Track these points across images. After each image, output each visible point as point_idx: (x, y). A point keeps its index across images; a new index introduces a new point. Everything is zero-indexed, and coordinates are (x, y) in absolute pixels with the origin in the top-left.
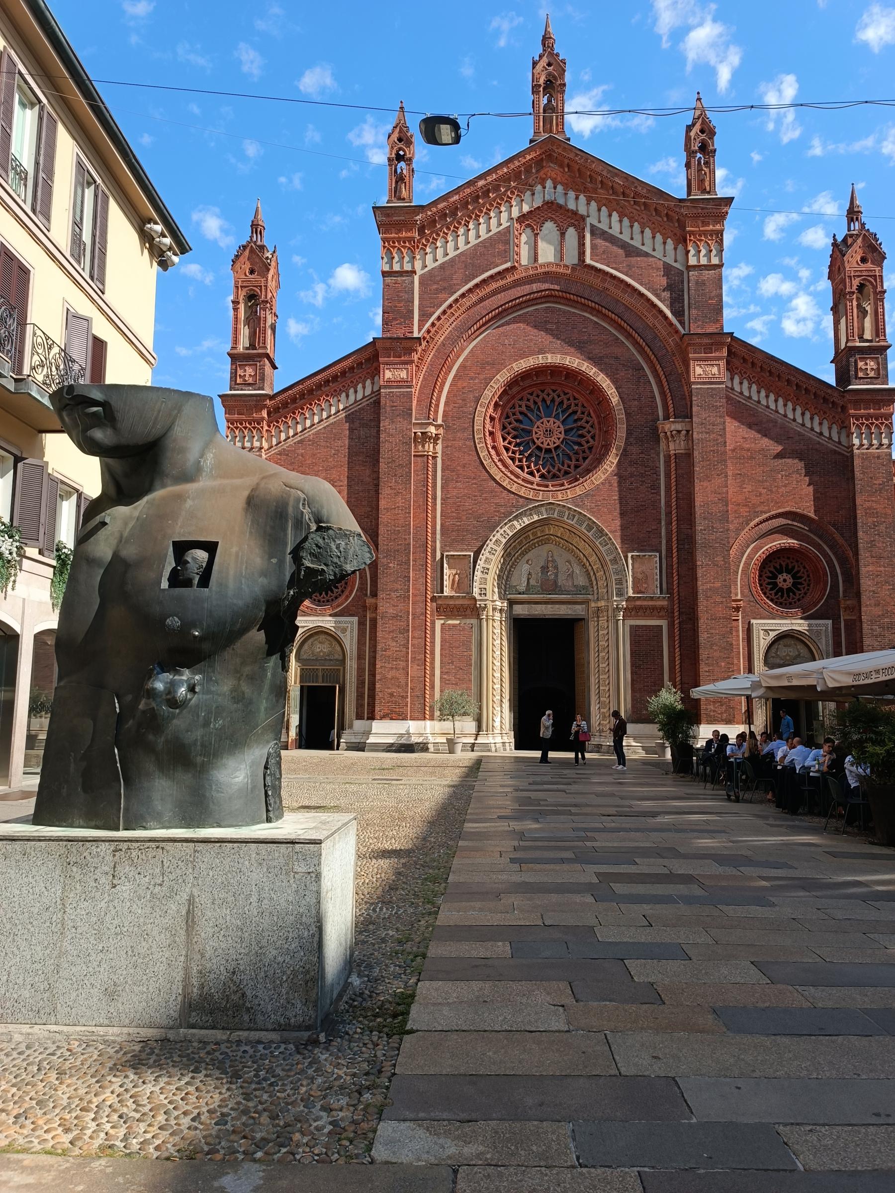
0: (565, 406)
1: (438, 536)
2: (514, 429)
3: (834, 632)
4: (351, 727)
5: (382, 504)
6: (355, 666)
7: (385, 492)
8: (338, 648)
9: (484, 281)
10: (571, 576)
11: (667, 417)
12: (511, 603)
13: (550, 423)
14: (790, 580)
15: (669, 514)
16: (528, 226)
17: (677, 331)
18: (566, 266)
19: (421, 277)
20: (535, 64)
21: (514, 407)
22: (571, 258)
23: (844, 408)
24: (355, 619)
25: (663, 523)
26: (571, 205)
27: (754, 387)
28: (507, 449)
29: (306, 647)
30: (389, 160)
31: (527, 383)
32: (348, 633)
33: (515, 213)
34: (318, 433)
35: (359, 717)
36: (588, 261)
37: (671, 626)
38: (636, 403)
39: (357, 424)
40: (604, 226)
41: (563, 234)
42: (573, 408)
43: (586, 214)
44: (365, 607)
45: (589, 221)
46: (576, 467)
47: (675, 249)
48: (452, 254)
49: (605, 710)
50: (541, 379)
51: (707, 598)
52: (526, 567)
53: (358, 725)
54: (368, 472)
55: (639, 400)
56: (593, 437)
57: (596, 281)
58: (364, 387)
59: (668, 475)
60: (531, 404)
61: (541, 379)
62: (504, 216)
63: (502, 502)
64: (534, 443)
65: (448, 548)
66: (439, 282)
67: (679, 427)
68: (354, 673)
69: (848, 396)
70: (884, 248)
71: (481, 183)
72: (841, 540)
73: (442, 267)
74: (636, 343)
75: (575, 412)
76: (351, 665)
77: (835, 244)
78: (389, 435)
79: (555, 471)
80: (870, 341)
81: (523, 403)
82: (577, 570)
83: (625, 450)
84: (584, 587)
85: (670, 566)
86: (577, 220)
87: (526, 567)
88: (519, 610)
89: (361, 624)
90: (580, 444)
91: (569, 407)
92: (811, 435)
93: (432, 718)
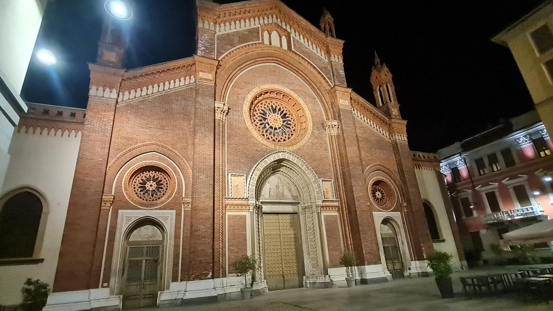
4: (168, 288)
19: (218, 36)
22: (285, 46)
24: (174, 212)
26: (284, 27)
32: (169, 220)
34: (155, 98)
35: (175, 279)
36: (293, 50)
39: (180, 98)
40: (297, 38)
41: (280, 37)
48: (233, 30)
49: (314, 262)
50: (272, 95)
51: (359, 201)
53: (176, 287)
60: (266, 106)
61: (272, 95)
64: (269, 125)
65: (230, 171)
68: (172, 248)
73: (228, 34)
76: (169, 244)
78: (201, 105)
81: (263, 106)
83: (312, 131)
84: (297, 197)
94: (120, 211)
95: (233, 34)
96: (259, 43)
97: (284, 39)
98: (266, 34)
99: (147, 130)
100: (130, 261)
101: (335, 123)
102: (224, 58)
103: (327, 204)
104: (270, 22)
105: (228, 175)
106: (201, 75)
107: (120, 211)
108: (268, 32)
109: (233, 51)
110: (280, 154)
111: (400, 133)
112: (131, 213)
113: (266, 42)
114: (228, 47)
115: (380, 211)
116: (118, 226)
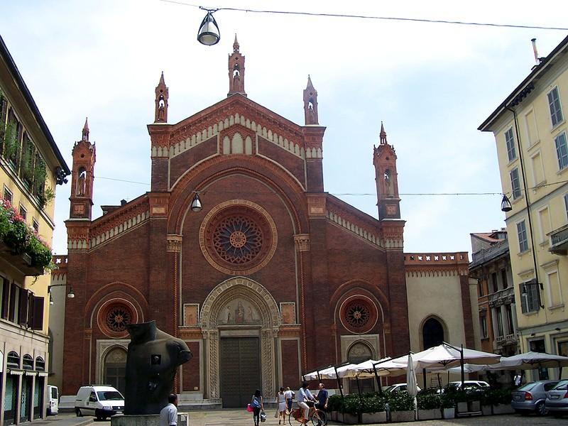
0: (247, 225)
1: (181, 295)
2: (220, 237)
3: (380, 341)
5: (152, 279)
10: (251, 315)
11: (298, 233)
13: (240, 234)
15: (299, 282)
17: (302, 190)
20: (230, 57)
21: (220, 226)
22: (249, 152)
23: (381, 229)
25: (297, 286)
26: (248, 126)
28: (216, 248)
29: (109, 356)
30: (156, 101)
31: (226, 214)
33: (221, 128)
37: (302, 340)
38: (282, 225)
39: (137, 236)
41: (244, 140)
43: (255, 130)
45: (257, 134)
46: (253, 257)
47: (300, 149)
48: (189, 148)
52: (227, 310)
56: (261, 242)
57: (262, 163)
58: (141, 217)
59: (299, 263)
62: (215, 129)
66: (181, 162)
67: (303, 238)
69: (383, 224)
72: (382, 295)
73: (182, 155)
74: (282, 195)
75: (251, 229)
77: (375, 149)
79: (241, 259)
80: (392, 197)
82: (254, 312)
84: (258, 321)
85: (300, 309)
86: (251, 133)
87: (227, 311)
88: (224, 333)
90: (255, 246)
95: (187, 153)
97: (248, 140)
99: (112, 272)
100: (107, 378)
101: (303, 237)
102: (178, 184)
103: (285, 329)
104: (232, 123)
105: (182, 305)
106: (155, 210)
108: (229, 137)
109: (187, 174)
110: (236, 281)
111: (393, 238)
112: (105, 342)
113: (226, 151)
114: (182, 170)
115: (352, 334)
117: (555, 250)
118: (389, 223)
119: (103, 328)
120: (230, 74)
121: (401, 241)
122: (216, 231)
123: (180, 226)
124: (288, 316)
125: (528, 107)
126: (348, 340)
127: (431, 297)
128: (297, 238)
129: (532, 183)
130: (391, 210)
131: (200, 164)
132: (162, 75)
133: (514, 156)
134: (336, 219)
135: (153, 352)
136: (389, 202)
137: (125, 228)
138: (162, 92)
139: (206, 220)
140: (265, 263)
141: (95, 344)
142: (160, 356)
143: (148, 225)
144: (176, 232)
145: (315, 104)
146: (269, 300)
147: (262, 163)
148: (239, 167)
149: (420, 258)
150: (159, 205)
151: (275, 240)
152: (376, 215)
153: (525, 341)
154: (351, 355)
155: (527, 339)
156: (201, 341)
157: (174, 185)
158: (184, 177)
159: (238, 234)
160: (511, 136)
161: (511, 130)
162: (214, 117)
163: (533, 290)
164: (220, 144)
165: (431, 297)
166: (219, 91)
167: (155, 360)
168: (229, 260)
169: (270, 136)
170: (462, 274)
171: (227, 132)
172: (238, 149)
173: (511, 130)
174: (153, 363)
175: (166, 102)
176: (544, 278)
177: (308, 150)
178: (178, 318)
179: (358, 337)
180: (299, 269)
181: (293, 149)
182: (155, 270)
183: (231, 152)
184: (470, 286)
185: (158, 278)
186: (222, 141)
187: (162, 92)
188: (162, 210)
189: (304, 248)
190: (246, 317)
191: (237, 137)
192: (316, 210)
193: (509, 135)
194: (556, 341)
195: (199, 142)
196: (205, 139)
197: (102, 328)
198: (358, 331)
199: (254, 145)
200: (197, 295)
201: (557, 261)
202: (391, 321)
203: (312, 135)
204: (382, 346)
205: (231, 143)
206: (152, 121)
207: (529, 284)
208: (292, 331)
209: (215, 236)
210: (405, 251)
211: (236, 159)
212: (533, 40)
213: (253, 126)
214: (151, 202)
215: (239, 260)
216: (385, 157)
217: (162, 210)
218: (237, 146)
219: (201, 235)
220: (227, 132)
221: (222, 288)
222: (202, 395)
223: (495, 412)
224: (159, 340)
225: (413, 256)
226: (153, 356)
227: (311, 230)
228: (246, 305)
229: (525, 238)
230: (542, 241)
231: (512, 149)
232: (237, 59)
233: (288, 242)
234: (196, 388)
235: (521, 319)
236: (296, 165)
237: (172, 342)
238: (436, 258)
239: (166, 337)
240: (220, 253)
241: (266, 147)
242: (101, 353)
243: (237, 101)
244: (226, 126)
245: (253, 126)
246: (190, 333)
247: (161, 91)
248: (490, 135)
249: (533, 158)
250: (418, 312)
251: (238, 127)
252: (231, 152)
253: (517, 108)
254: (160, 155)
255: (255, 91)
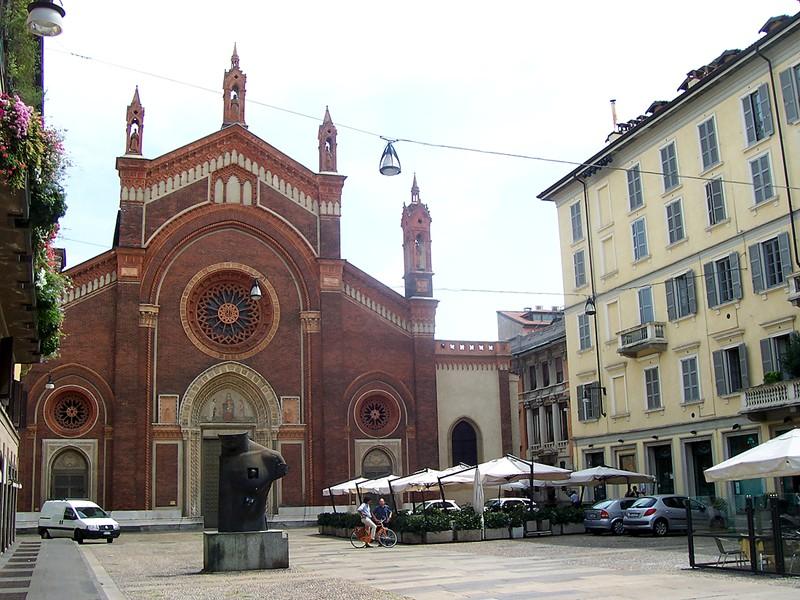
2: (206, 309)
5: (119, 360)
6: (96, 474)
7: (121, 352)
8: (82, 461)
9: (190, 211)
10: (242, 410)
12: (203, 428)
13: (230, 307)
14: (378, 414)
16: (220, 177)
18: (244, 207)
21: (205, 294)
22: (248, 201)
23: (409, 310)
26: (248, 168)
27: (358, 293)
28: (201, 323)
33: (213, 169)
41: (242, 185)
42: (245, 297)
43: (257, 174)
44: (103, 432)
46: (247, 337)
48: (170, 191)
54: (107, 337)
55: (288, 296)
56: (258, 318)
57: (264, 217)
62: (205, 170)
63: (198, 361)
66: (161, 209)
70: (432, 215)
71: (190, 149)
72: (407, 390)
73: (161, 199)
75: (246, 300)
76: (93, 474)
81: (212, 292)
82: (246, 406)
86: (252, 177)
88: (208, 433)
89: (101, 444)
91: (242, 296)
92: (390, 324)
93: (150, 509)
94: (44, 440)
95: (168, 198)
96: (205, 205)
97: (248, 186)
98: (219, 183)
100: (56, 489)
101: (313, 315)
104: (227, 163)
106: (124, 271)
107: (44, 440)
109: (167, 226)
111: (422, 321)
113: (219, 198)
115: (369, 438)
116: (44, 456)
117: (625, 352)
118: (417, 301)
119: (52, 424)
120: (226, 96)
121: (432, 325)
122: (201, 301)
123: (155, 293)
124: (290, 414)
125: (602, 180)
126: (363, 445)
127: (466, 396)
128: (304, 315)
129: (600, 272)
130: (421, 285)
131: (185, 214)
132: (137, 91)
133: (580, 234)
134: (354, 294)
135: (249, 465)
136: (419, 276)
137: (83, 293)
138: (135, 114)
139: (190, 286)
140: (263, 345)
141: (40, 444)
142: (257, 469)
143: (115, 290)
144: (149, 301)
145: (333, 145)
146: (268, 393)
147: (264, 217)
148: (234, 220)
149: (452, 347)
150: (131, 264)
151: (277, 316)
152: (402, 292)
153: (580, 452)
154: (365, 465)
155: (583, 451)
156: (180, 443)
157: (150, 240)
158: (163, 230)
159: (229, 309)
160: (579, 211)
161: (578, 204)
162: (204, 152)
163: (593, 394)
164: (211, 190)
165: (466, 396)
166: (211, 121)
167: (252, 474)
168: (217, 340)
169: (275, 183)
170: (501, 369)
171: (221, 174)
172: (233, 196)
173: (578, 204)
174: (250, 477)
175: (141, 127)
176: (608, 382)
177: (323, 204)
178: (151, 413)
179: (376, 442)
180: (306, 356)
181: (305, 202)
182: (124, 350)
183: (225, 200)
184: (510, 384)
185: (127, 360)
186: (213, 185)
187: (135, 114)
188: (134, 272)
189: (313, 328)
190: (237, 413)
191: (233, 181)
192: (330, 282)
193: (575, 209)
194: (618, 454)
195: (185, 185)
196: (192, 181)
197: (50, 424)
198: (377, 435)
199: (254, 193)
200: (176, 384)
201: (625, 364)
202: (416, 423)
203: (328, 185)
204: (404, 454)
205: (225, 188)
206: (122, 152)
207: (589, 388)
208: (295, 433)
209: (199, 308)
210: (437, 337)
211: (231, 210)
212: (613, 101)
213: (254, 168)
214: (119, 260)
215: (228, 340)
216: (416, 224)
217: (134, 272)
218: (233, 192)
219: (183, 305)
220: (217, 174)
221: (209, 375)
222: (180, 512)
223: (564, 532)
224: (252, 452)
225: (444, 344)
226: (250, 469)
227: (323, 306)
228: (236, 397)
229: (587, 332)
230: (608, 339)
231: (577, 225)
232: (236, 77)
233: (292, 319)
234: (173, 503)
235: (577, 428)
236: (307, 222)
237: (267, 454)
238: (472, 348)
239: (260, 449)
240: (205, 330)
241: (270, 196)
242: (48, 456)
243: (235, 133)
244: (220, 166)
245: (254, 168)
246: (167, 432)
247: (136, 112)
248: (551, 205)
249: (604, 242)
250: (448, 415)
251: (235, 169)
252: (225, 200)
253: (588, 180)
254: (132, 198)
255: (257, 122)
